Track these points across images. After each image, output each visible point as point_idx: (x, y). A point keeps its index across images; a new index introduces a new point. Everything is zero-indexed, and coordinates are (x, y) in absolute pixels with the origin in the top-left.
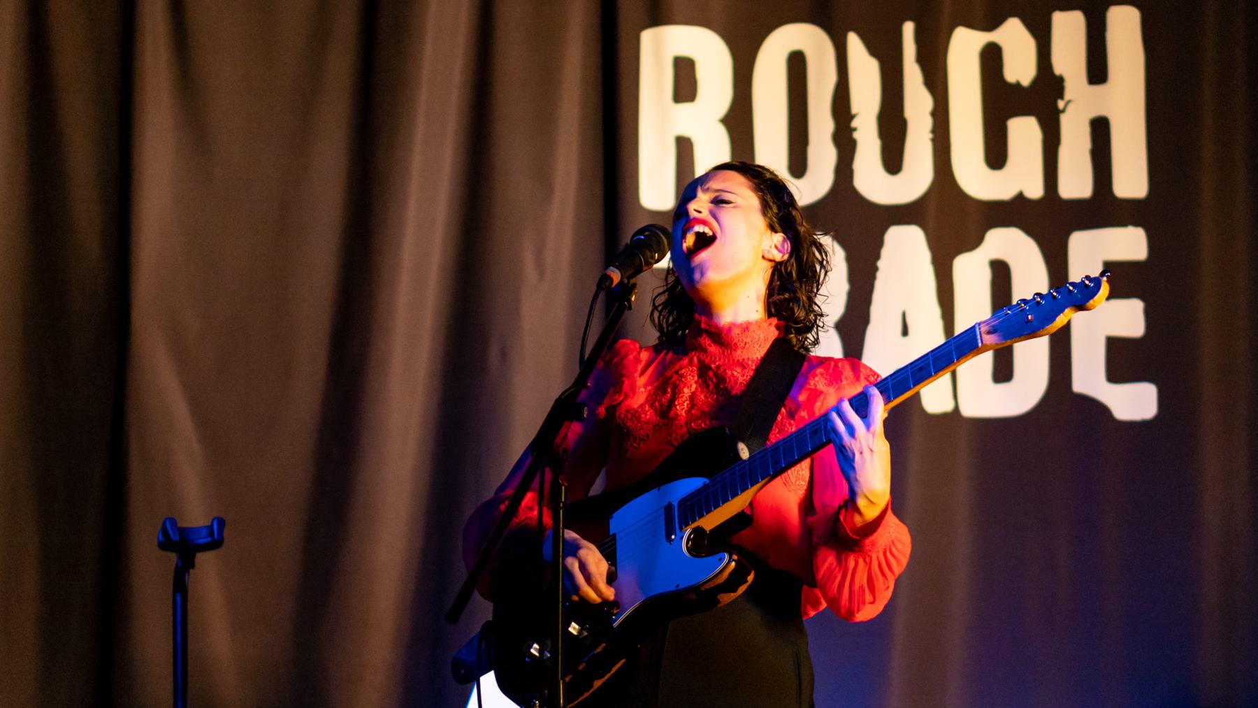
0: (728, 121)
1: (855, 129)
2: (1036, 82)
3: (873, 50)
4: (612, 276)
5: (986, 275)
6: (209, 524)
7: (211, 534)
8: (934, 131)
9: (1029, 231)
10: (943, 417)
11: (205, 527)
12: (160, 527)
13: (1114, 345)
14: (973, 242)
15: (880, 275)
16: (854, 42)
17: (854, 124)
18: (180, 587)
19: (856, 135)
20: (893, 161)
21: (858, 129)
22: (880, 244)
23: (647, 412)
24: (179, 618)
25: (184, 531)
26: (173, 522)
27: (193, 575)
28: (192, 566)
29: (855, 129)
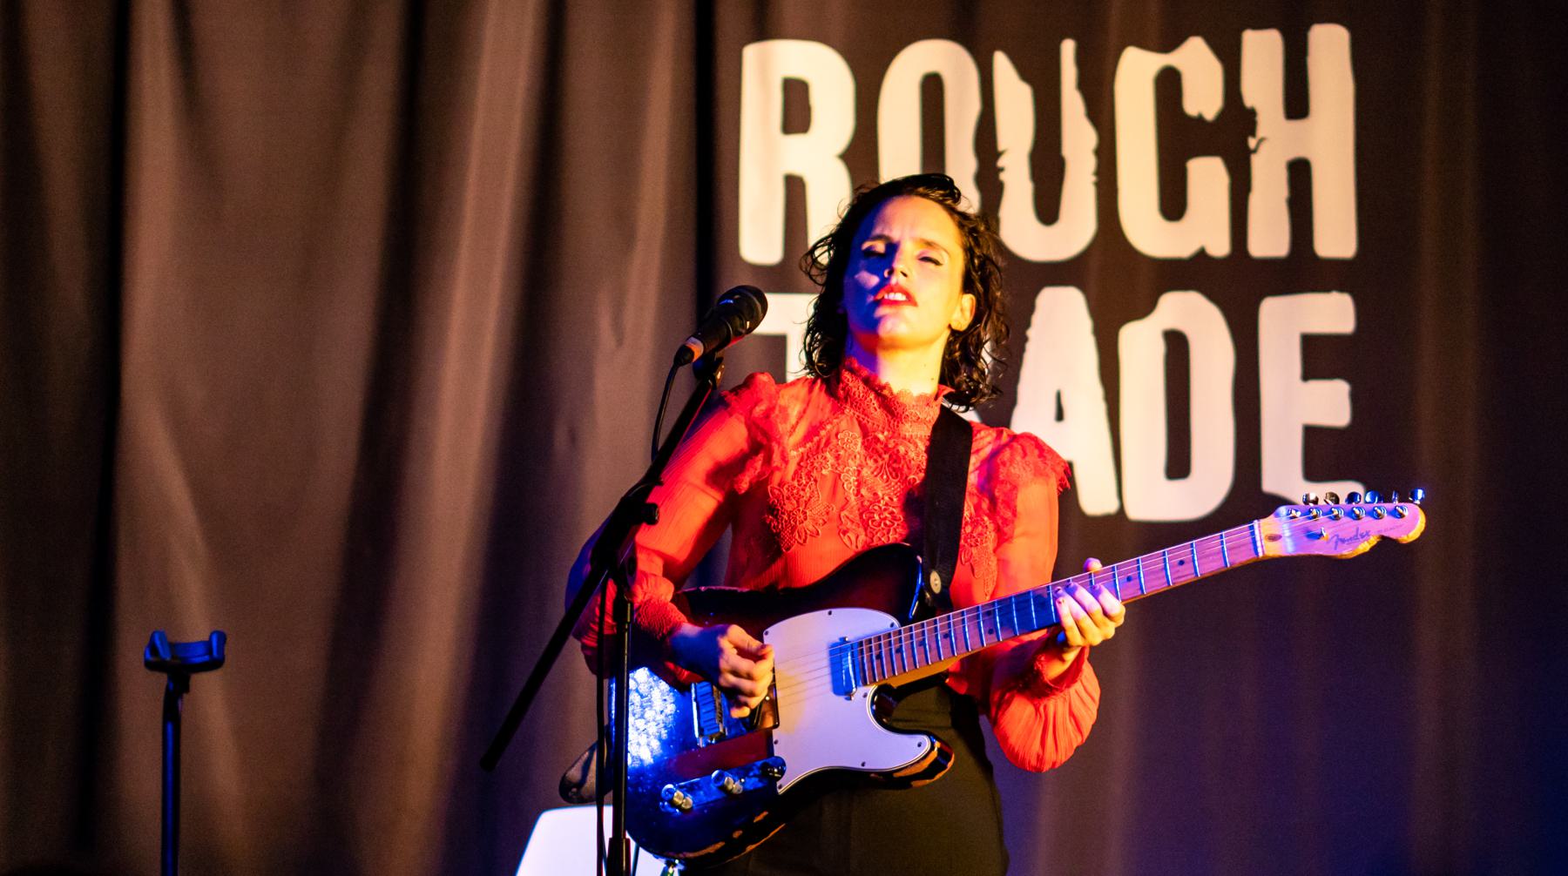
0: (848, 157)
1: (1002, 170)
2: (1222, 115)
3: (1025, 74)
4: (693, 348)
5: (1159, 349)
6: (204, 637)
7: (209, 651)
8: (1098, 173)
9: (1212, 296)
10: (1105, 520)
11: (203, 643)
12: (147, 642)
13: (1315, 437)
14: (1145, 308)
15: (1031, 348)
16: (1001, 62)
17: (1001, 163)
18: (172, 715)
19: (1003, 176)
20: (1047, 209)
21: (1006, 169)
22: (1030, 309)
23: (805, 486)
24: (170, 752)
25: (174, 646)
26: (162, 635)
27: (186, 703)
28: (186, 689)
29: (1002, 170)
